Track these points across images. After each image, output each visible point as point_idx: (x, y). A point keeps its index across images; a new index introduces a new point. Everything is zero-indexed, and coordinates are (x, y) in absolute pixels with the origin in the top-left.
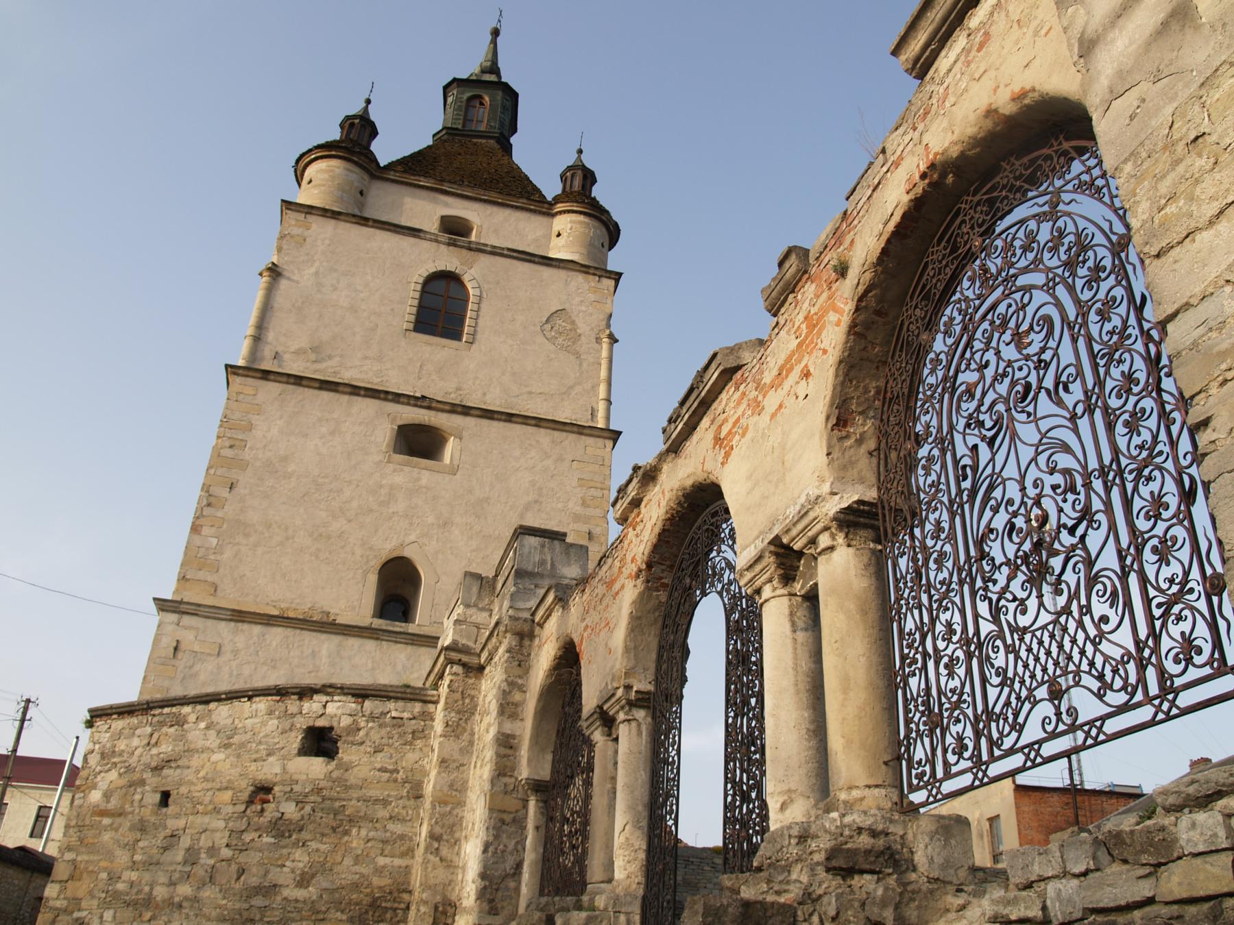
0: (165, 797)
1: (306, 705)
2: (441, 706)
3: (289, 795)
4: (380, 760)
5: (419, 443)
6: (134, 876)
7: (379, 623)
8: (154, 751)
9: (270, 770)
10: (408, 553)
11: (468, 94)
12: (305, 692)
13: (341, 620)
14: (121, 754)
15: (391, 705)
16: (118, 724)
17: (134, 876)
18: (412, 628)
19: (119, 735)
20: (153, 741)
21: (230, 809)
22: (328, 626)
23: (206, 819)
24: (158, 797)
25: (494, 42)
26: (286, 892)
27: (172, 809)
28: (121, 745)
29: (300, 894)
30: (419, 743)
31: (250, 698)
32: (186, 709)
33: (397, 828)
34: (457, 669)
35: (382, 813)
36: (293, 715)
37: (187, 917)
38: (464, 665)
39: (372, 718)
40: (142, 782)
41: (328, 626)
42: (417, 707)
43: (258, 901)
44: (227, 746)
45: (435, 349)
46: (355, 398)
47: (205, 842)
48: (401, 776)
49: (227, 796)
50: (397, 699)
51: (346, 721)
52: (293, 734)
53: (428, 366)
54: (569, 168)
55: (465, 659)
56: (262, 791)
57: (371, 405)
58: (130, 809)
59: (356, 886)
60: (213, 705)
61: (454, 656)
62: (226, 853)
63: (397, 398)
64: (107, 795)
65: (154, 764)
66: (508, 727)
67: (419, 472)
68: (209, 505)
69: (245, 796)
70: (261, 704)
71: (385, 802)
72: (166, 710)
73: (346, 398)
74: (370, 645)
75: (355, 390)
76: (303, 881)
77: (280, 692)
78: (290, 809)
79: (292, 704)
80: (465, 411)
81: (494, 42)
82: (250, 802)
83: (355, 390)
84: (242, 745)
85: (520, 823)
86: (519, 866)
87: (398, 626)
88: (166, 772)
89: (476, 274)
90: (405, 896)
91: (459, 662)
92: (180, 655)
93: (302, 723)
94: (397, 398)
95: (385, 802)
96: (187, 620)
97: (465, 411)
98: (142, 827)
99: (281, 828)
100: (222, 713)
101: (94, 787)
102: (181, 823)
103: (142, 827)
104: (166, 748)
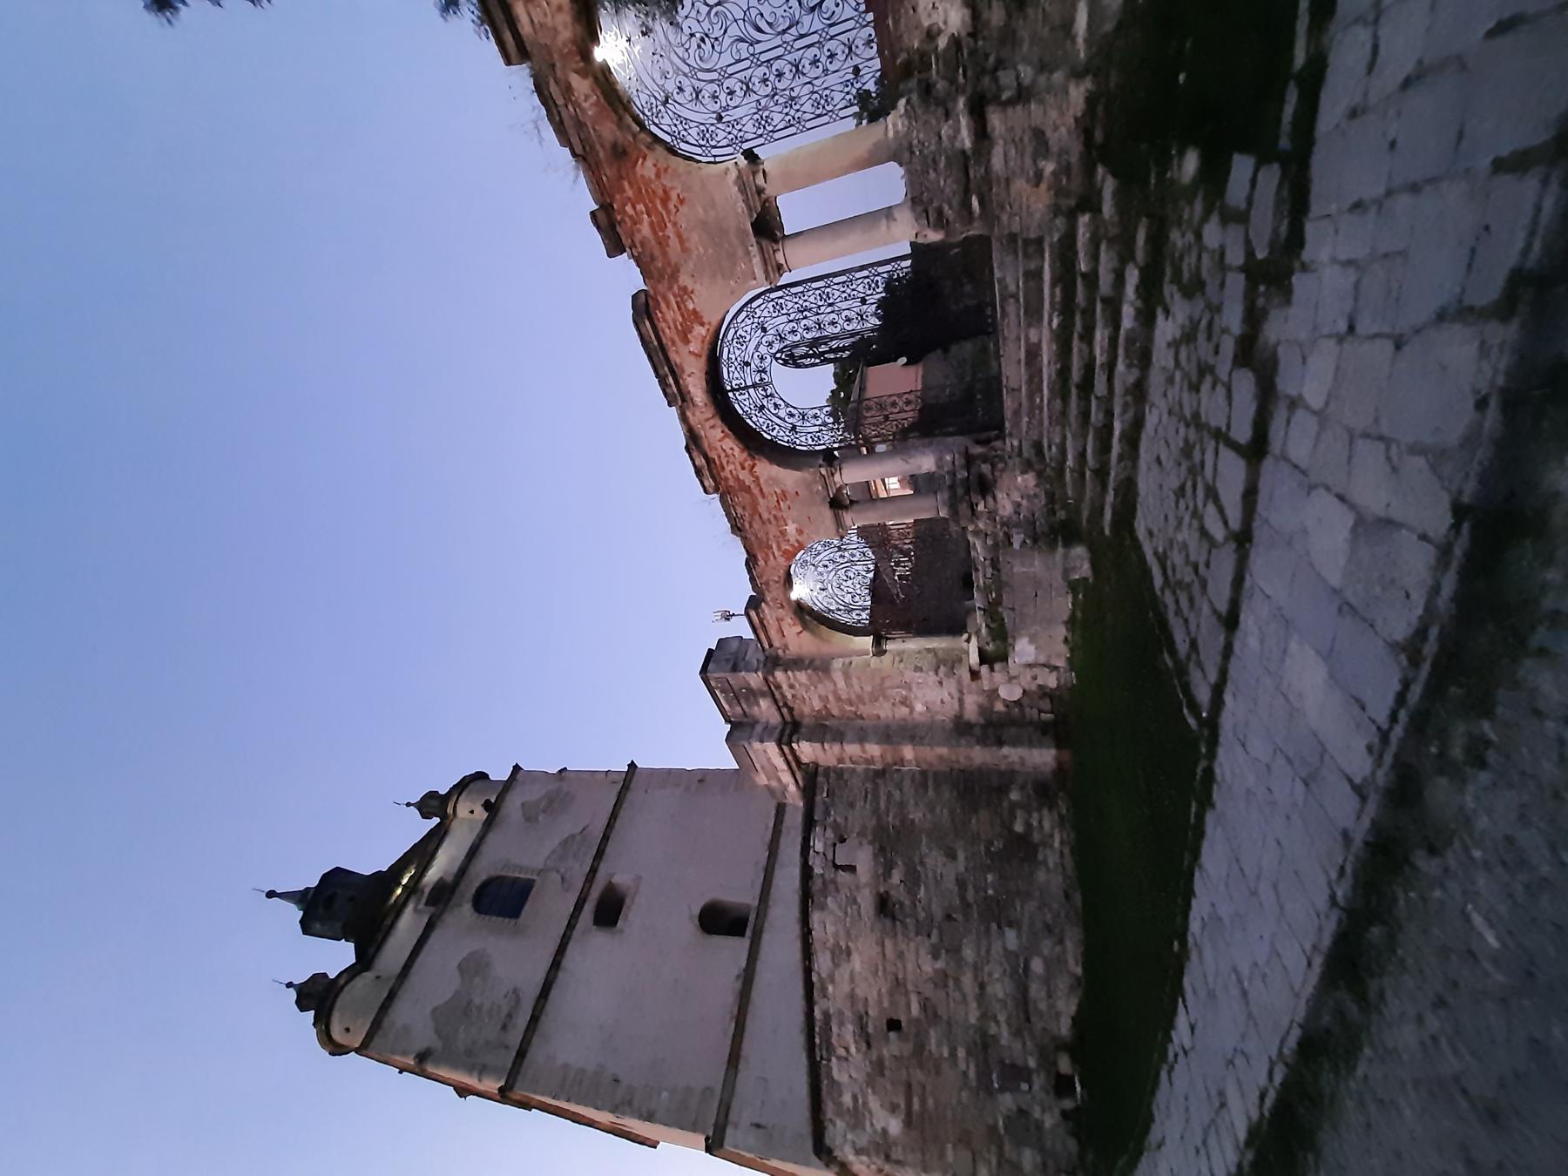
0: (894, 1025)
1: (817, 870)
3: (887, 874)
5: (610, 910)
6: (961, 1053)
7: (748, 933)
8: (853, 1049)
9: (866, 901)
10: (697, 911)
13: (744, 964)
14: (855, 1098)
15: (818, 798)
16: (829, 1109)
17: (961, 1053)
19: (839, 1105)
20: (841, 1052)
21: (900, 937)
22: (748, 976)
23: (910, 966)
24: (892, 1035)
26: (962, 869)
27: (903, 1019)
28: (847, 1099)
30: (846, 776)
32: (817, 1013)
33: (907, 783)
35: (897, 794)
36: (824, 883)
37: (990, 975)
39: (827, 813)
41: (748, 976)
42: (820, 779)
43: (970, 895)
44: (849, 954)
47: (929, 966)
48: (869, 786)
49: (888, 943)
51: (830, 833)
52: (839, 879)
53: (551, 907)
56: (884, 906)
57: (572, 949)
58: (904, 1072)
60: (814, 979)
61: (785, 739)
63: (571, 926)
64: (893, 1109)
65: (864, 1046)
67: (633, 918)
68: (630, 1103)
69: (888, 923)
70: (816, 917)
71: (889, 795)
72: (817, 1041)
73: (561, 974)
74: (766, 937)
75: (556, 965)
76: (952, 855)
79: (817, 885)
80: (593, 870)
82: (894, 919)
83: (556, 965)
85: (901, 653)
86: (929, 650)
88: (870, 1030)
89: (482, 871)
91: (790, 736)
92: (763, 1122)
93: (830, 875)
94: (571, 926)
95: (889, 795)
96: (733, 1116)
97: (593, 870)
100: (822, 963)
101: (885, 1131)
102: (914, 999)
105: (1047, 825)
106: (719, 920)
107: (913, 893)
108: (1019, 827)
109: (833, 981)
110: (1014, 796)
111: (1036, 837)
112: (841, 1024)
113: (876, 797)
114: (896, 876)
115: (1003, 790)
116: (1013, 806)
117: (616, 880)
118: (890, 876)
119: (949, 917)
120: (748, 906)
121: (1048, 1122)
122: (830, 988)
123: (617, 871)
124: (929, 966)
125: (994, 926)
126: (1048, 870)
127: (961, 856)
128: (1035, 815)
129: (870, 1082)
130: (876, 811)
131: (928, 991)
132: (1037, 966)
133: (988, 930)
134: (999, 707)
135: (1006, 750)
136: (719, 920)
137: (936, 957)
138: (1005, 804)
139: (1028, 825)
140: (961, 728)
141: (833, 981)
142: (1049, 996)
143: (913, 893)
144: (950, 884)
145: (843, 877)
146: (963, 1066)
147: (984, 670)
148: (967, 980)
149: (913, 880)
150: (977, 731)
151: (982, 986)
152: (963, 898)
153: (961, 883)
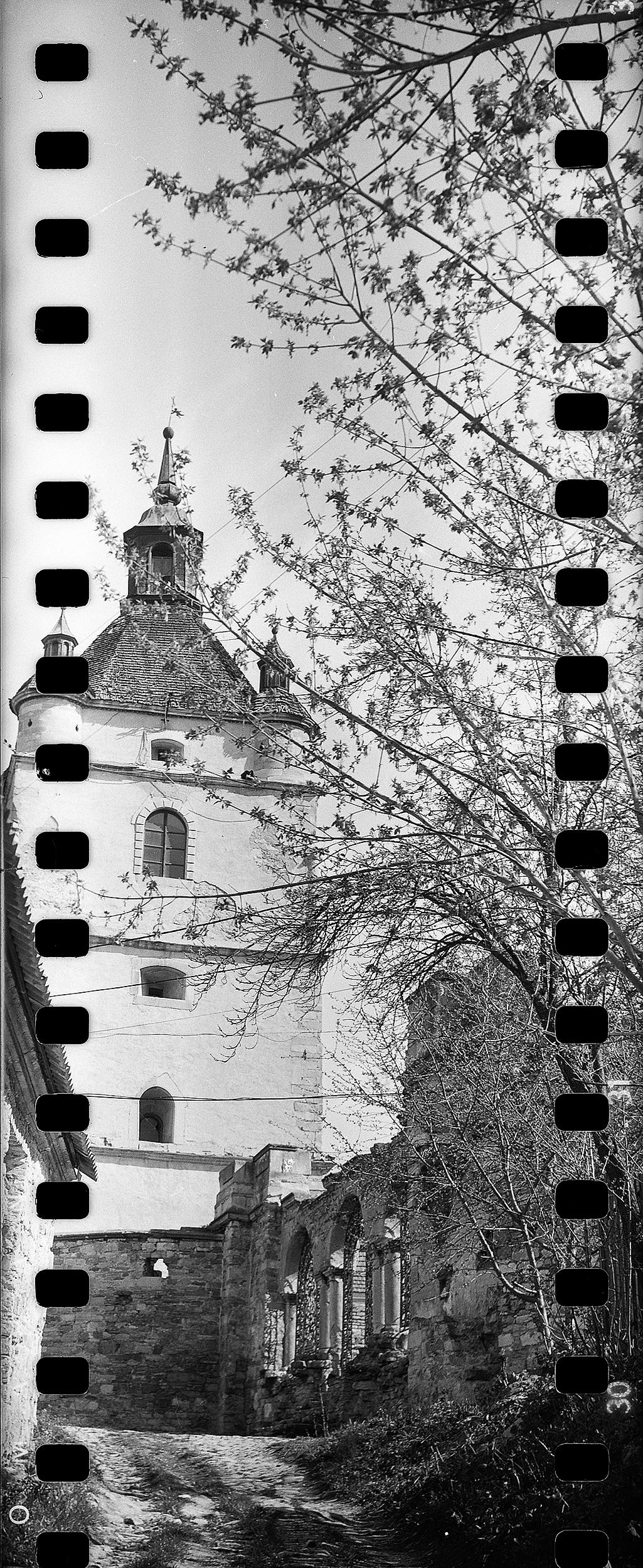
4: (192, 1278)
9: (127, 1284)
12: (141, 1237)
29: (155, 1357)
31: (105, 1239)
33: (207, 1318)
34: (236, 1223)
38: (240, 1221)
42: (212, 1245)
43: (132, 1362)
47: (90, 1328)
50: (199, 1240)
51: (170, 1254)
55: (240, 1218)
56: (124, 1297)
59: (186, 1352)
61: (234, 1216)
62: (105, 1334)
66: (272, 1265)
70: (114, 1244)
76: (157, 1351)
78: (142, 1307)
79: (136, 1246)
84: (106, 1269)
90: (217, 1357)
91: (237, 1220)
95: (199, 1303)
99: (141, 1320)
107: (133, 1320)
108: (176, 1401)
109: (79, 1257)
110: (200, 1402)
113: (197, 1293)
114: (142, 1307)
115: (204, 1393)
116: (192, 1400)
118: (142, 1302)
119: (118, 1346)
122: (73, 1255)
124: (90, 1328)
126: (148, 1419)
127: (155, 1357)
128: (185, 1415)
130: (187, 1292)
133: (110, 1372)
134: (252, 1392)
135: (225, 1396)
137: (97, 1334)
138: (192, 1394)
141: (79, 1257)
142: (77, 1412)
143: (133, 1320)
144: (138, 1348)
145: (141, 1266)
147: (261, 1381)
150: (240, 1375)
152: (130, 1356)
153: (138, 1357)
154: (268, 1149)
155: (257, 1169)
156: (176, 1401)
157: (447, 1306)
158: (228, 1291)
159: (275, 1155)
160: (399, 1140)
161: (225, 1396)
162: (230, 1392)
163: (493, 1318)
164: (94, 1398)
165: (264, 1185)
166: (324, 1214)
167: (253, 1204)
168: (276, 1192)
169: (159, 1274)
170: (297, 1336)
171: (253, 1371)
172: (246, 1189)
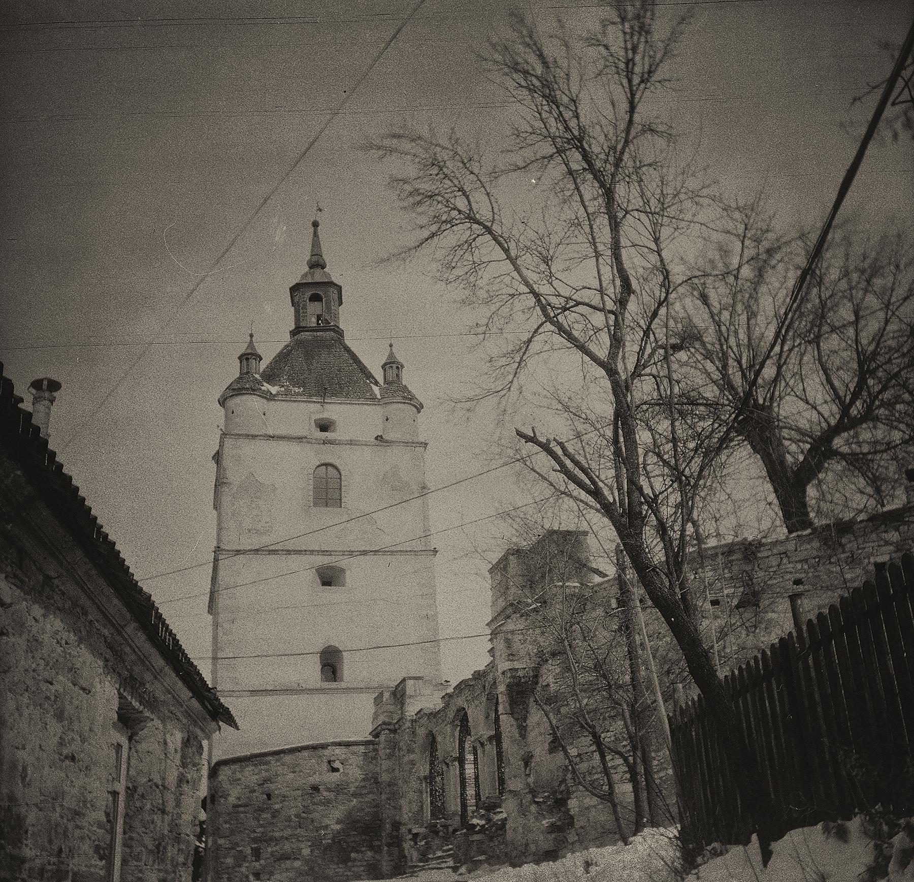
0: (269, 797)
1: (327, 752)
2: (382, 746)
3: (329, 790)
5: (329, 578)
7: (326, 685)
9: (315, 779)
11: (308, 294)
12: (324, 746)
14: (240, 779)
18: (343, 685)
25: (315, 234)
28: (239, 775)
30: (374, 762)
39: (354, 753)
40: (255, 791)
44: (294, 772)
45: (328, 516)
46: (289, 557)
47: (293, 812)
49: (299, 792)
54: (385, 364)
56: (315, 788)
77: (314, 748)
79: (320, 752)
80: (351, 553)
81: (315, 234)
87: (333, 685)
88: (266, 785)
97: (351, 553)
98: (261, 810)
100: (288, 758)
103: (261, 810)
104: (264, 774)
105: (355, 869)
106: (331, 663)
108: (353, 855)
110: (369, 854)
111: (350, 864)
112: (267, 771)
115: (371, 848)
117: (348, 573)
120: (342, 680)
121: (243, 870)
123: (356, 572)
125: (310, 844)
128: (359, 864)
129: (246, 787)
131: (283, 813)
132: (297, 864)
136: (331, 663)
137: (297, 816)
138: (364, 849)
139: (355, 860)
140: (396, 825)
143: (320, 803)
145: (325, 767)
146: (258, 830)
147: (410, 836)
148: (288, 832)
149: (328, 802)
150: (395, 833)
151: (286, 838)
153: (326, 827)
154: (404, 680)
155: (399, 694)
156: (353, 855)
157: (531, 780)
158: (385, 777)
159: (410, 683)
160: (492, 666)
161: (386, 848)
162: (389, 845)
163: (563, 787)
164: (298, 859)
165: (403, 704)
166: (443, 721)
167: (396, 718)
168: (411, 710)
169: (337, 770)
170: (431, 803)
171: (403, 830)
172: (392, 708)
